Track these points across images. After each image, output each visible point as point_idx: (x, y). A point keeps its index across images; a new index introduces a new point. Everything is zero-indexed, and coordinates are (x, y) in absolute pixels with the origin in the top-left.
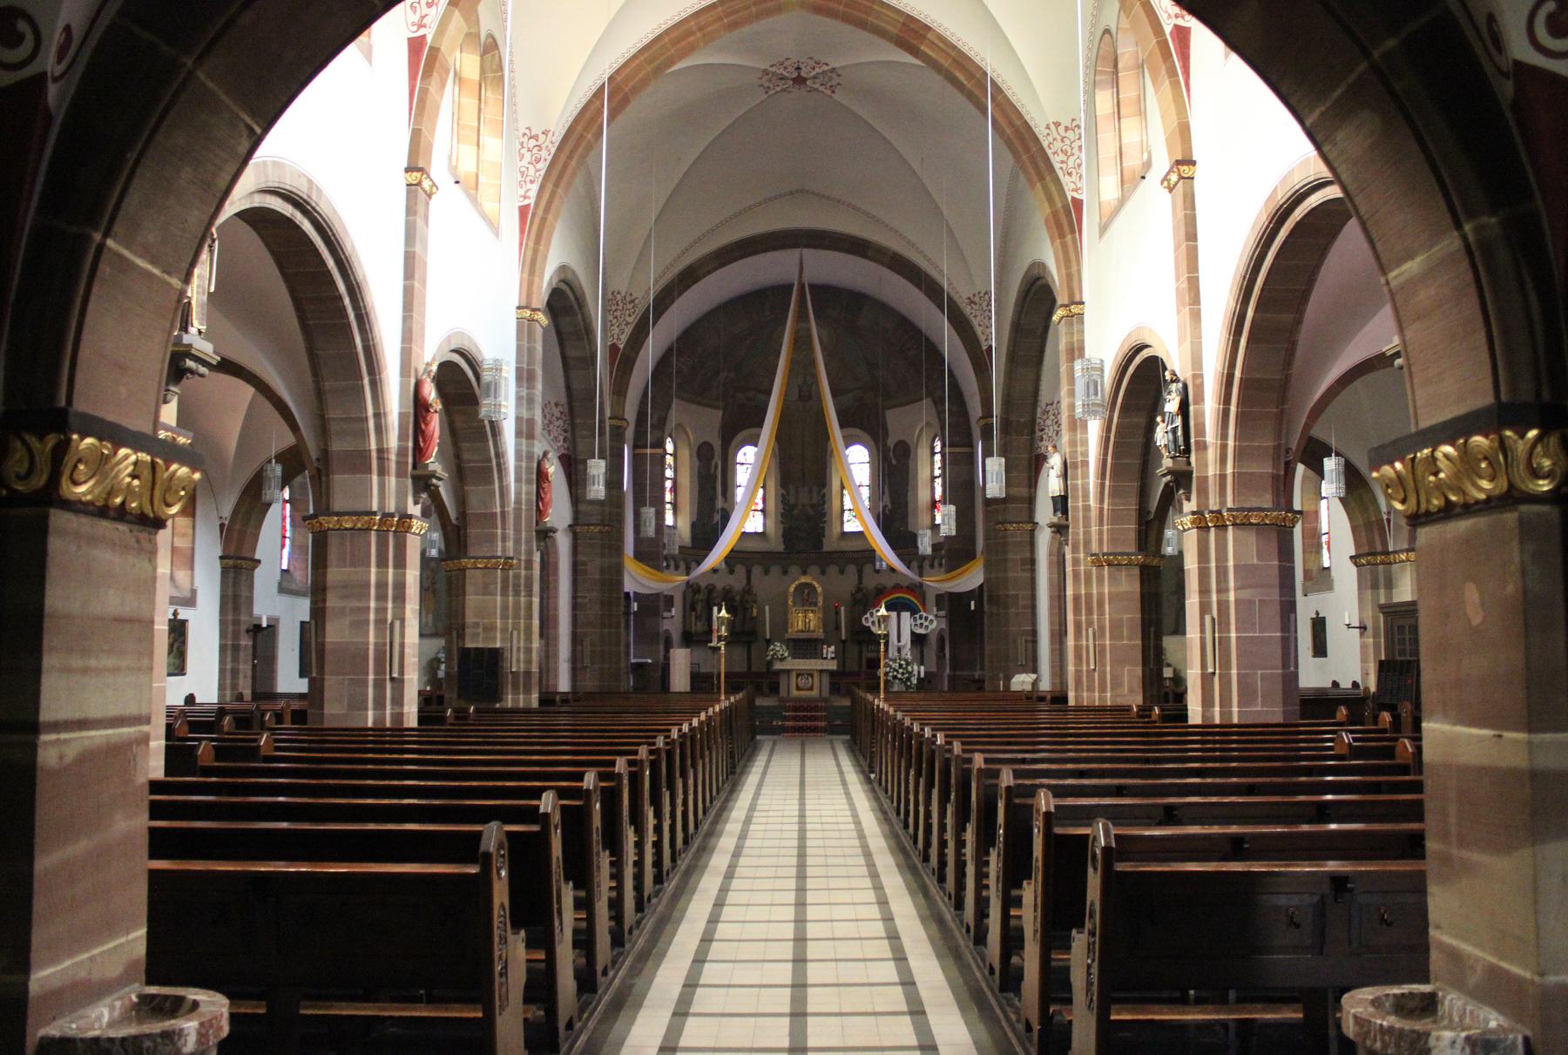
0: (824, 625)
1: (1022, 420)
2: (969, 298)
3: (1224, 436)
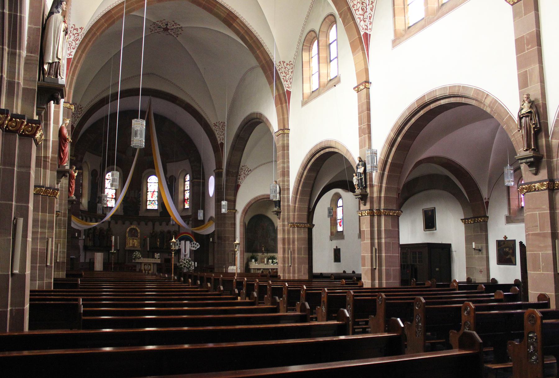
1: (234, 171)
2: (214, 124)
3: (381, 182)
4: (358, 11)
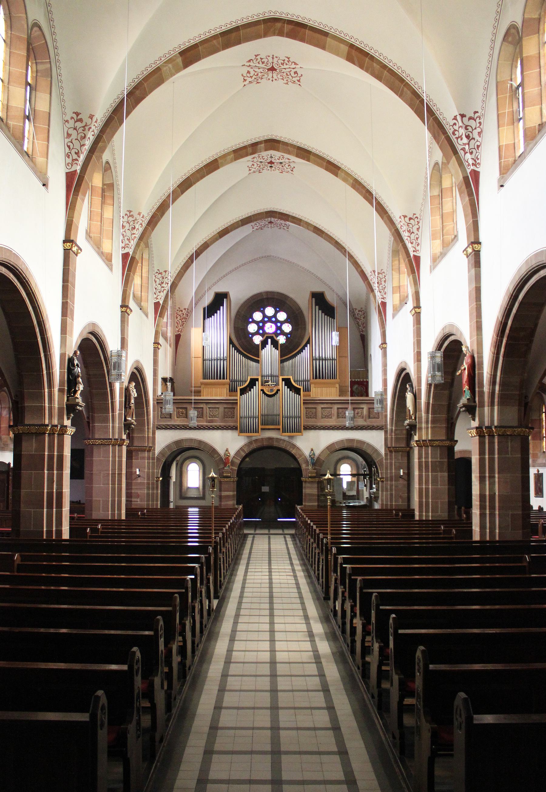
4: (461, 140)
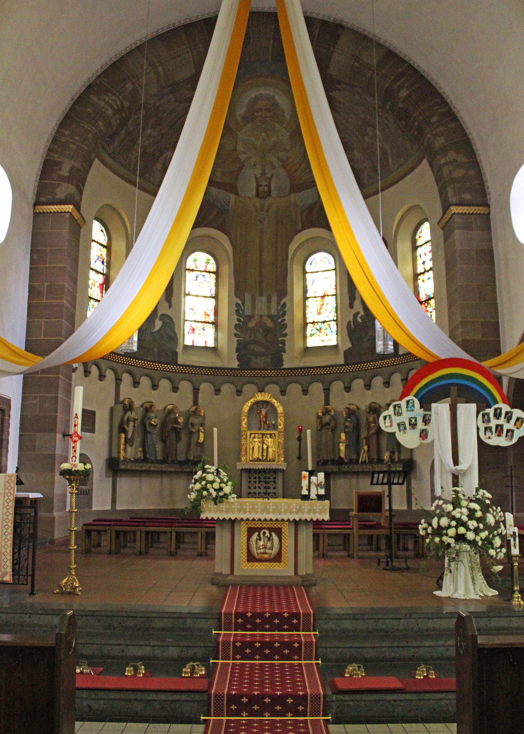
0: (285, 452)
